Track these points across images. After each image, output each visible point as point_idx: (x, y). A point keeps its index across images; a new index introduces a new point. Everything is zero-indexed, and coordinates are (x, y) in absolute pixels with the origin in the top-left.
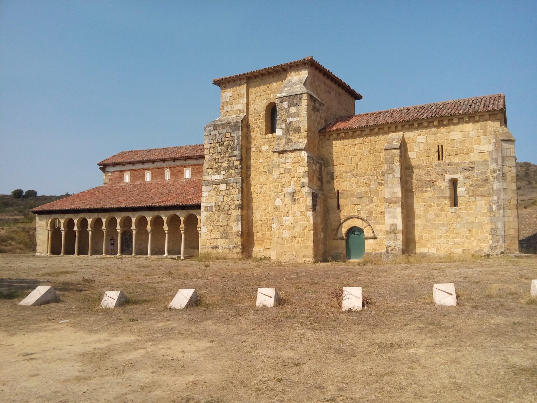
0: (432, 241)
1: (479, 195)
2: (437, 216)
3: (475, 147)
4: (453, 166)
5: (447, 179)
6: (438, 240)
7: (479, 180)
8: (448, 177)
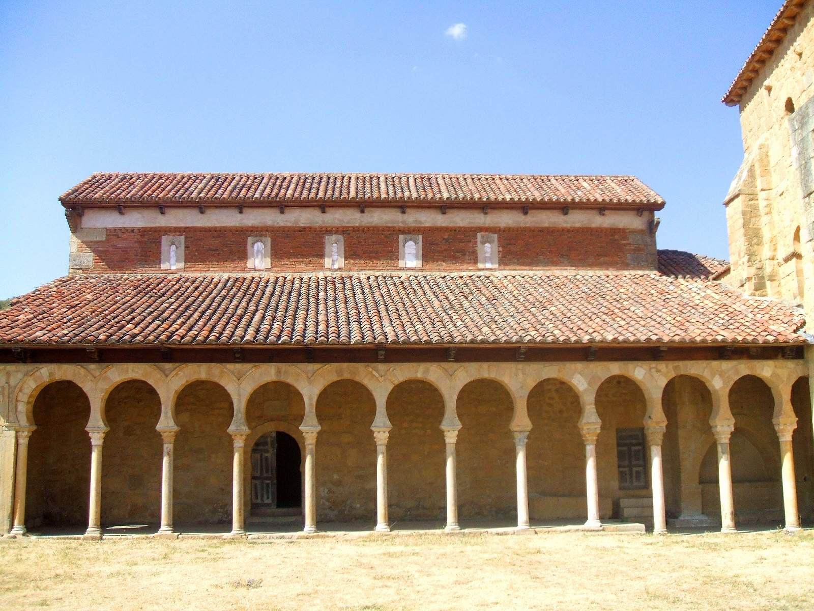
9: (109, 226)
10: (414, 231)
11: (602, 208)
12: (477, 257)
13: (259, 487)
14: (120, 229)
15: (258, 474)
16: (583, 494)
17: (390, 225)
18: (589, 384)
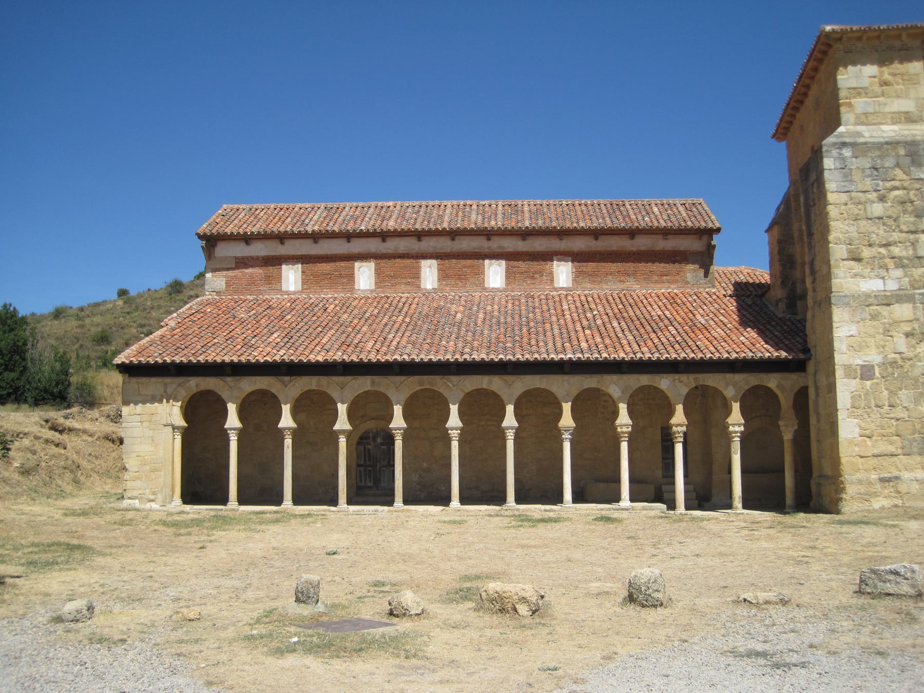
9: (239, 255)
10: (497, 255)
11: (666, 233)
12: (553, 278)
13: (363, 474)
14: (247, 258)
15: (362, 462)
16: (618, 481)
17: (477, 251)
18: (623, 392)
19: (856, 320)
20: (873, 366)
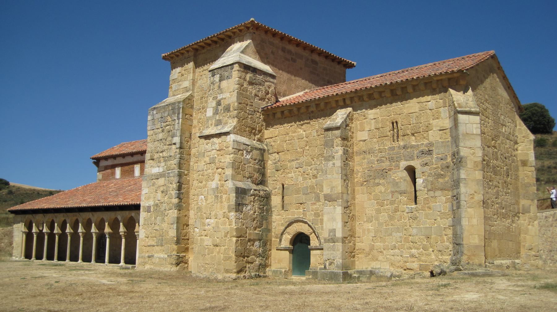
0: (384, 252)
1: (438, 189)
2: (391, 218)
3: (434, 122)
4: (409, 150)
5: (402, 167)
6: (392, 251)
7: (438, 167)
8: (404, 164)
9: (105, 165)
19: (148, 186)
20: (151, 206)
